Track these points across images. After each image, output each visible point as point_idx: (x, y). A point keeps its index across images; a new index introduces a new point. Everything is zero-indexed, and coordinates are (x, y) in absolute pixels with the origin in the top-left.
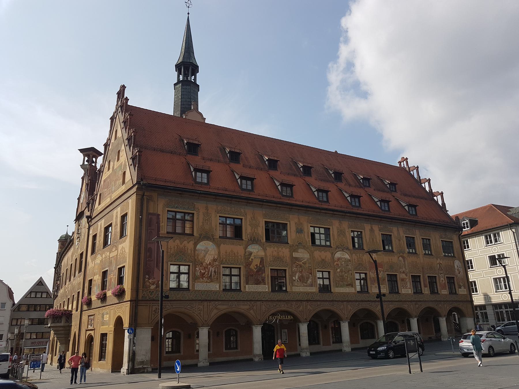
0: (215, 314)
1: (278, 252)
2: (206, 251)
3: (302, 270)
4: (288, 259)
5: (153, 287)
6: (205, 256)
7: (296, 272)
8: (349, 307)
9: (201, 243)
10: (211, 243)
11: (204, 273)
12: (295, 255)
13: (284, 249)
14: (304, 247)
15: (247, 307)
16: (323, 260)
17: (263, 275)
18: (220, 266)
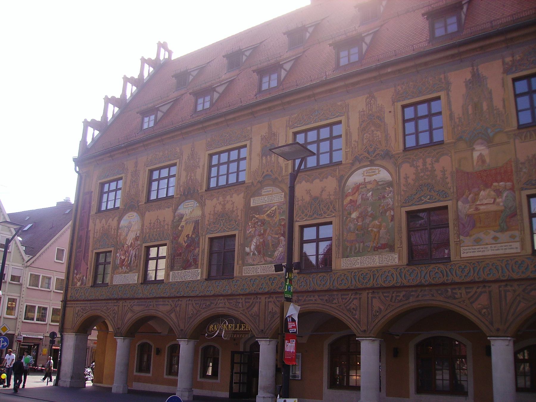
0: (130, 318)
1: (224, 205)
2: (129, 227)
3: (265, 231)
4: (239, 214)
5: (79, 284)
6: (127, 235)
7: (253, 237)
8: (376, 304)
9: (126, 217)
10: (135, 214)
11: (124, 259)
12: (255, 202)
13: (235, 195)
14: (275, 182)
15: (168, 308)
16: (315, 199)
17: (197, 249)
18: (141, 245)
